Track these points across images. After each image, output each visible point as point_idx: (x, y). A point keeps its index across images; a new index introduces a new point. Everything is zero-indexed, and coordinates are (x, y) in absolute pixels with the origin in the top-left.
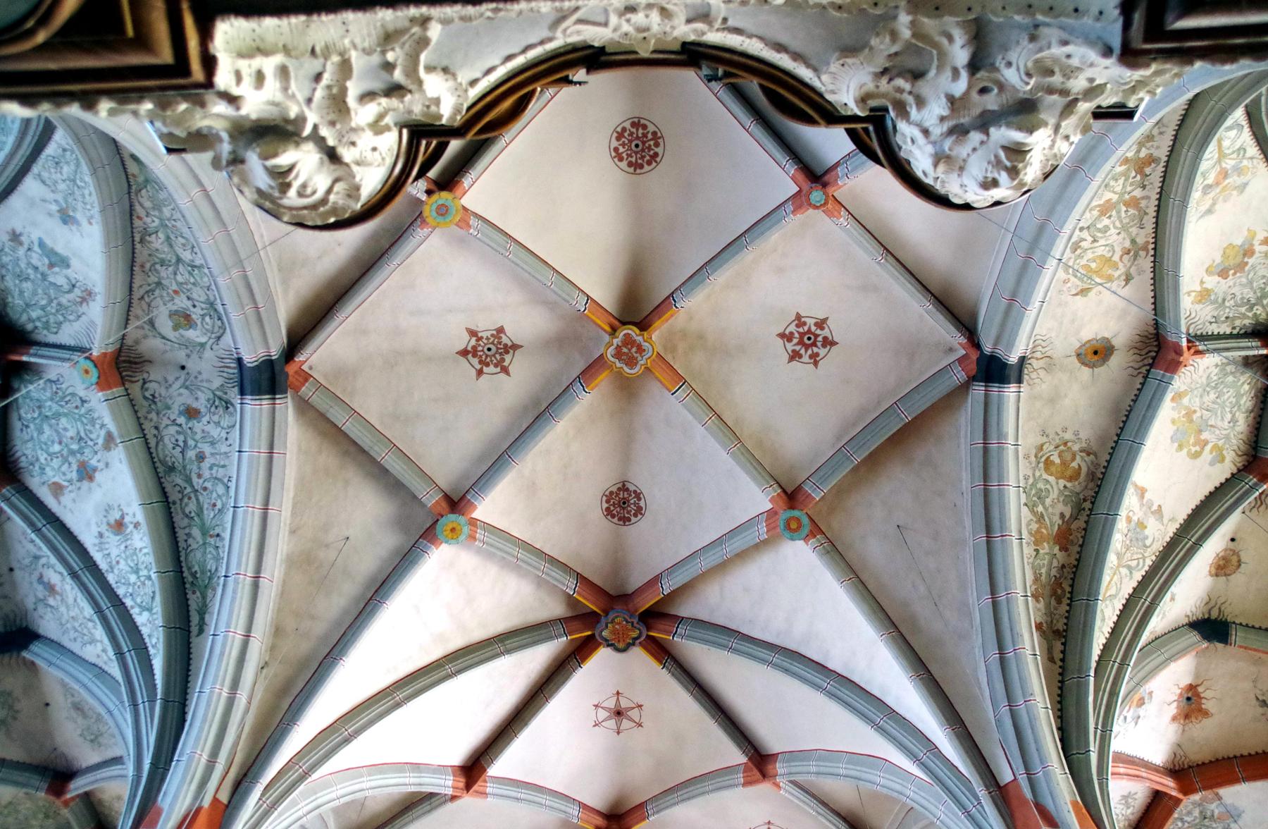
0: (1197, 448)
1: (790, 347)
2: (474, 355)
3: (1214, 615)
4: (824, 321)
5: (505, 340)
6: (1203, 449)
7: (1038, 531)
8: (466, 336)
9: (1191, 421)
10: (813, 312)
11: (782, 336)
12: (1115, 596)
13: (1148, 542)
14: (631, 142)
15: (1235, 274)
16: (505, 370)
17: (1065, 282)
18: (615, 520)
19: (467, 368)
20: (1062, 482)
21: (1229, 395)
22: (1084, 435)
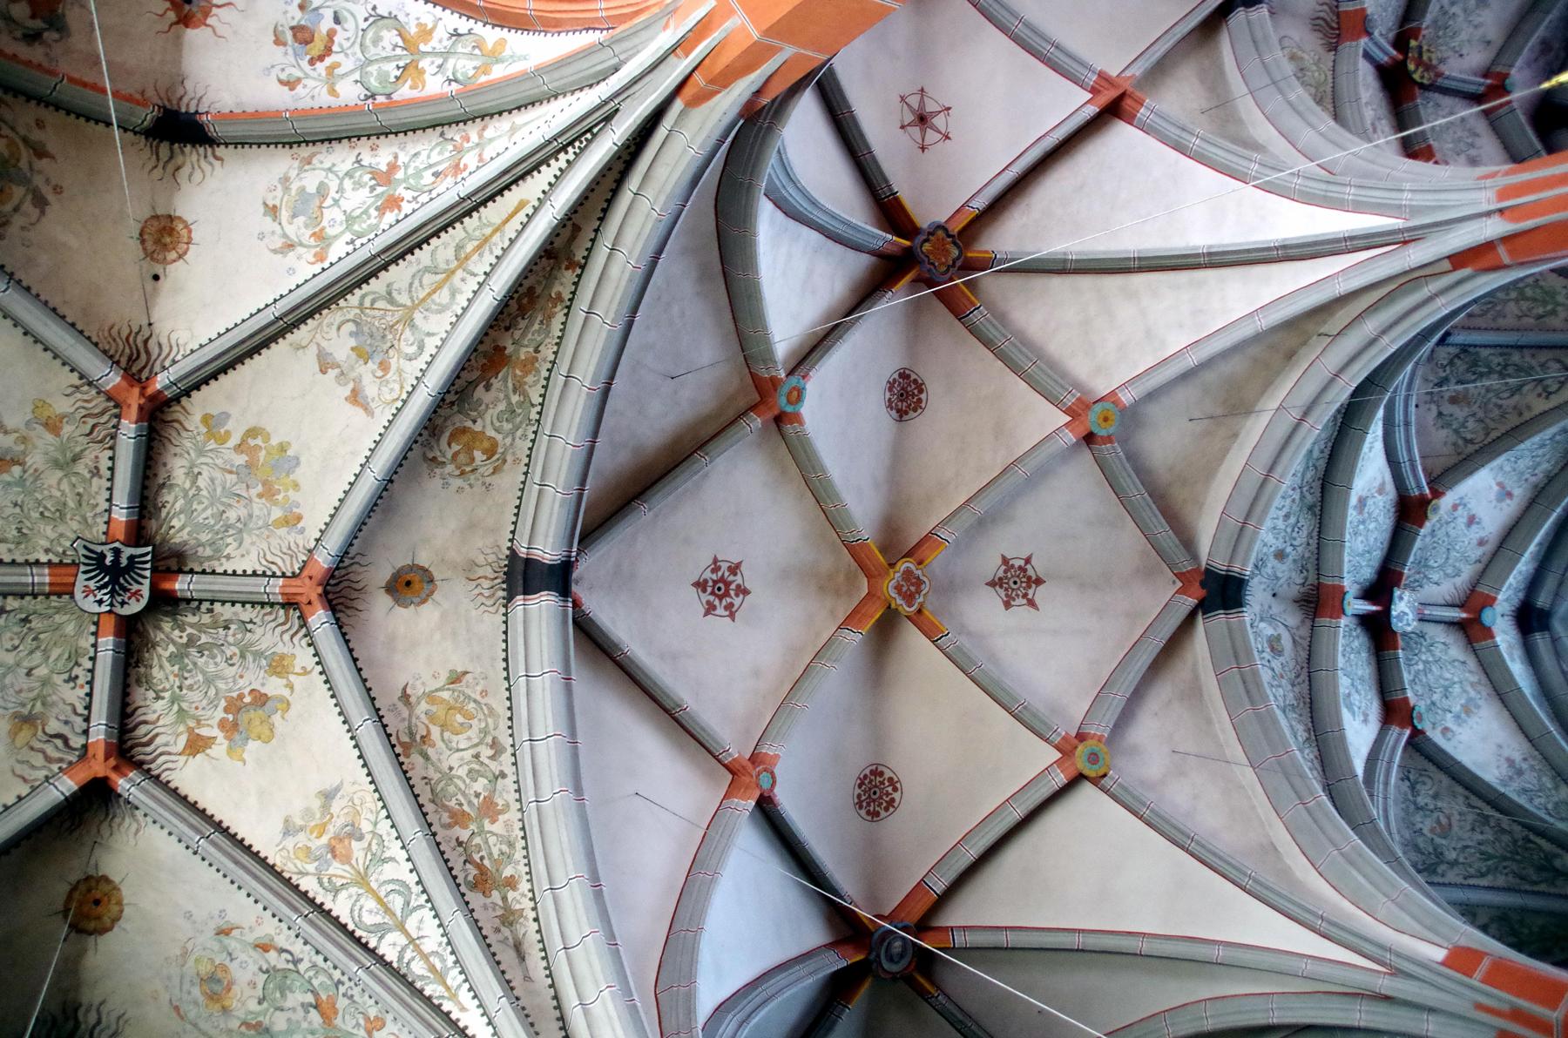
0: (252, 442)
2: (1029, 578)
3: (164, 149)
6: (243, 441)
7: (527, 373)
8: (1037, 600)
9: (264, 483)
12: (427, 270)
13: (350, 327)
15: (241, 697)
16: (1005, 561)
17: (484, 693)
18: (913, 377)
19: (1039, 567)
20: (478, 427)
21: (205, 514)
22: (437, 482)
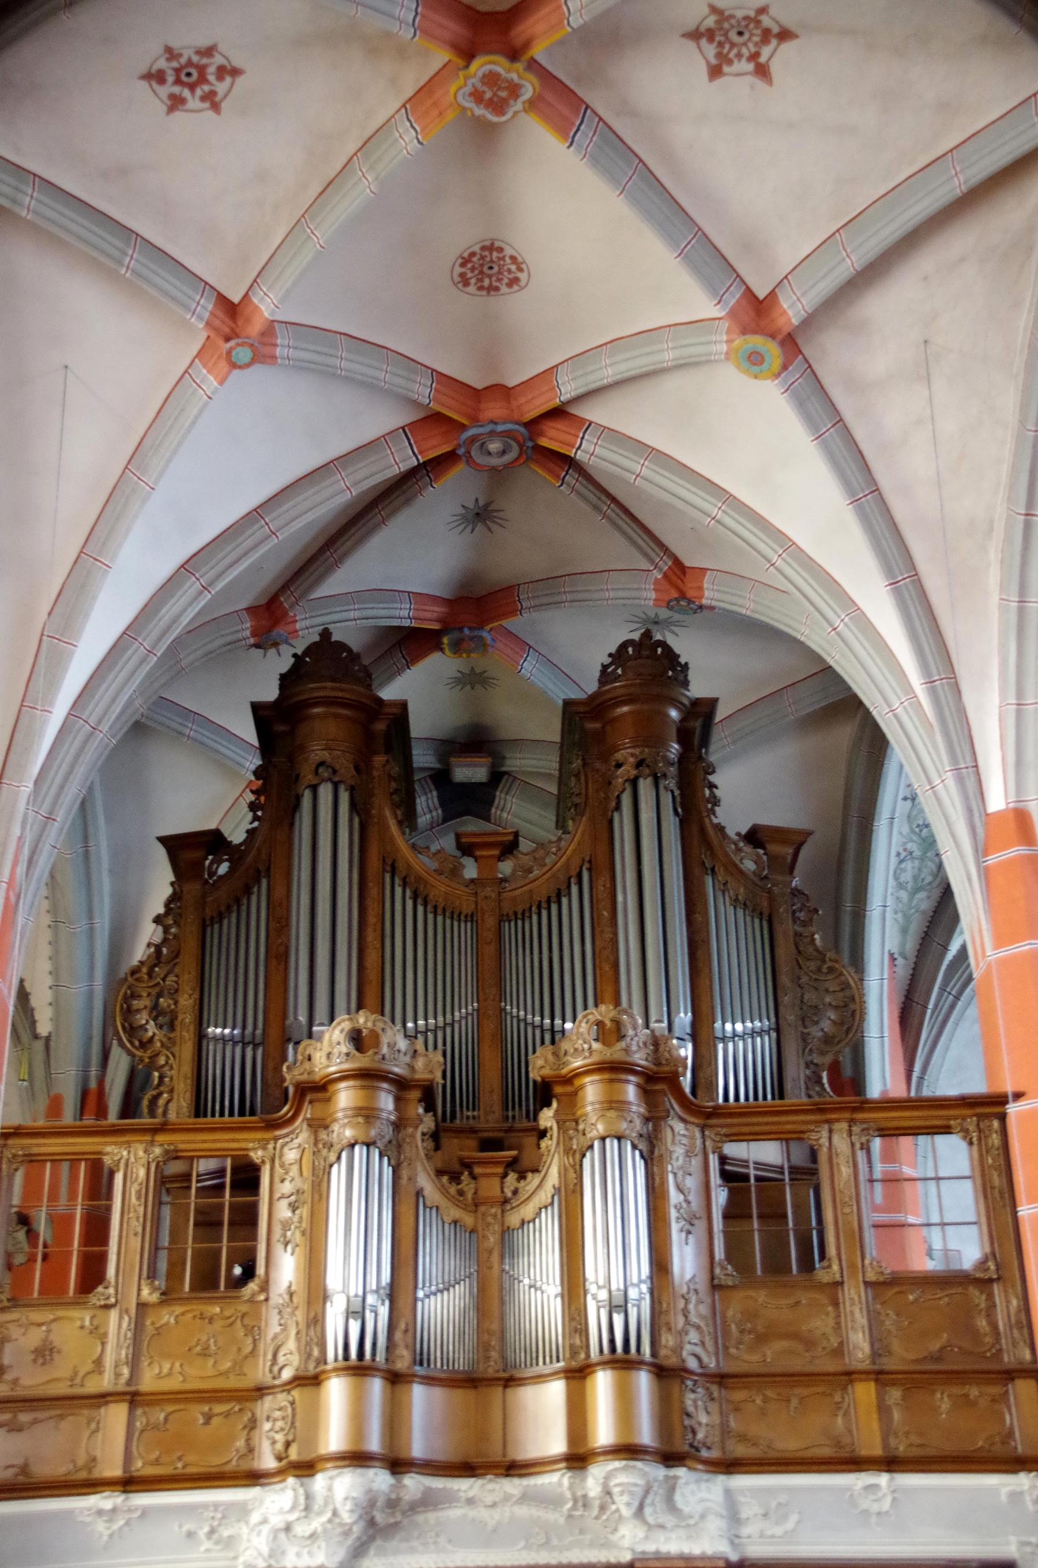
1: (218, 60)
4: (171, 109)
5: (710, 50)
8: (775, 68)
10: (195, 120)
11: (235, 72)
14: (500, 272)
